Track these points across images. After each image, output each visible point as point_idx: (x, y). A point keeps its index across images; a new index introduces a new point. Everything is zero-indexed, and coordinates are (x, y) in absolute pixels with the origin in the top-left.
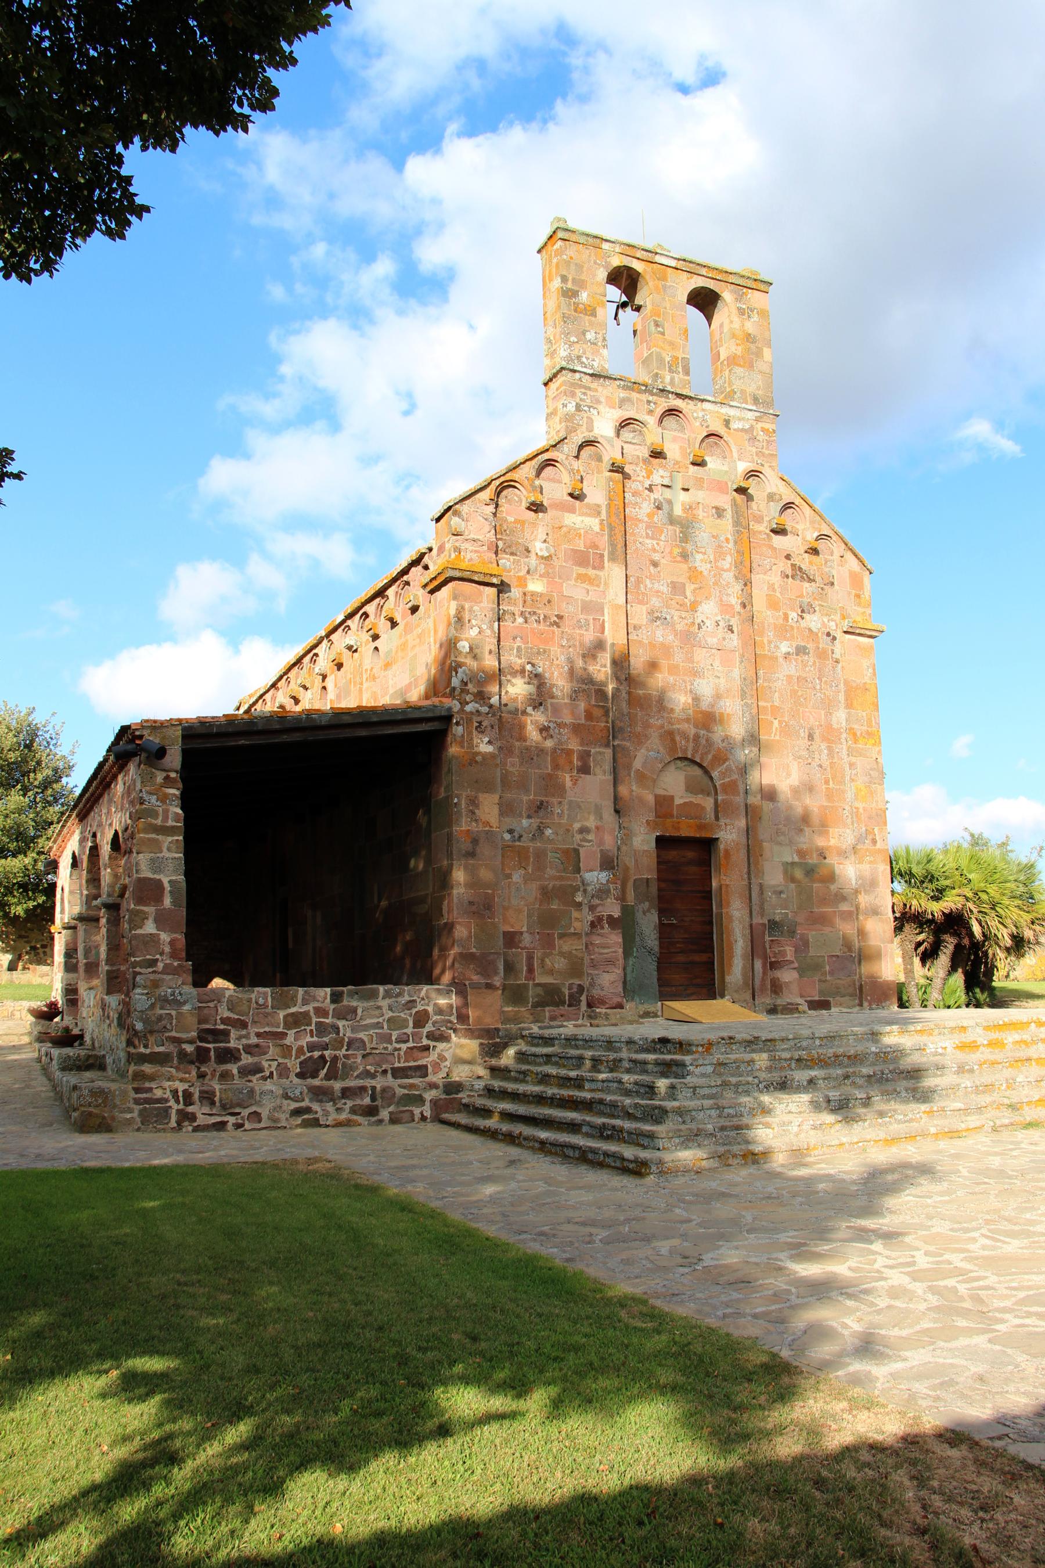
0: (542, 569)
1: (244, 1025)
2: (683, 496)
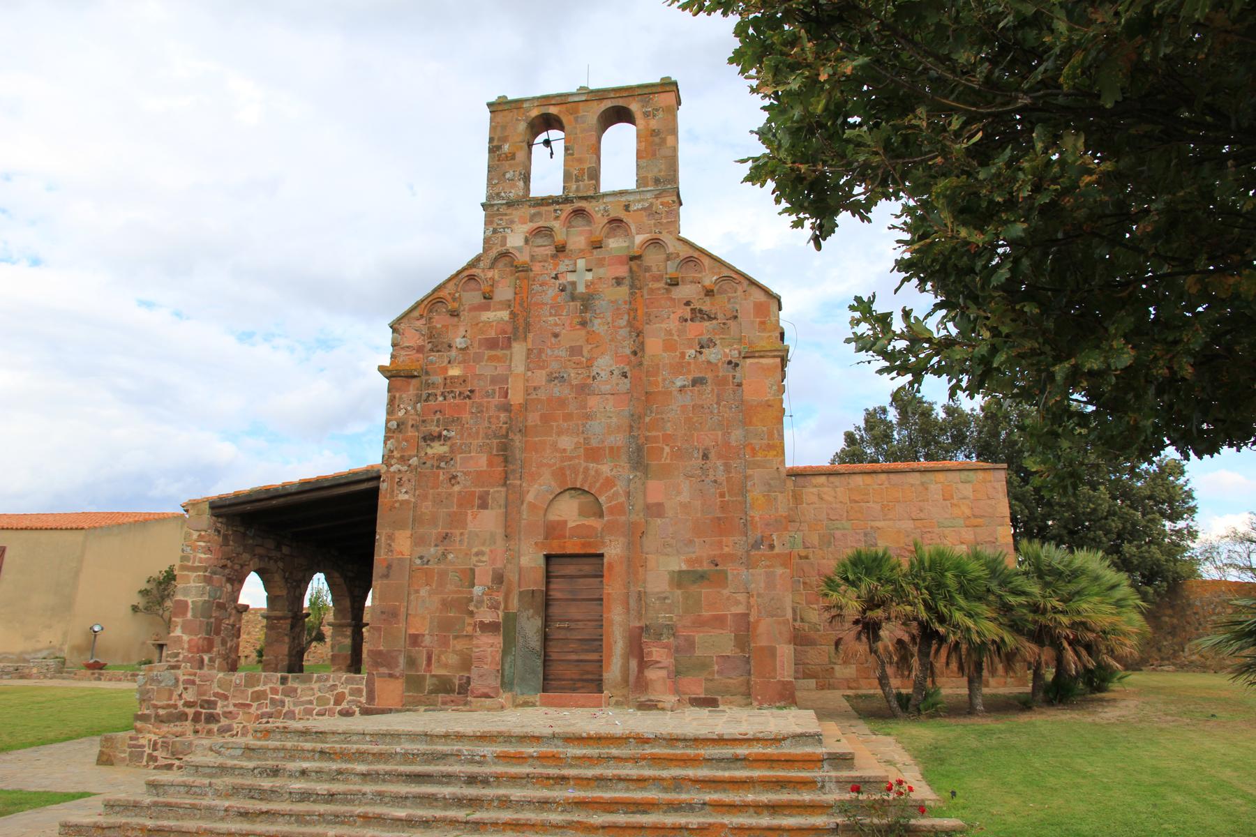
0: (460, 358)
1: (226, 698)
2: (589, 276)
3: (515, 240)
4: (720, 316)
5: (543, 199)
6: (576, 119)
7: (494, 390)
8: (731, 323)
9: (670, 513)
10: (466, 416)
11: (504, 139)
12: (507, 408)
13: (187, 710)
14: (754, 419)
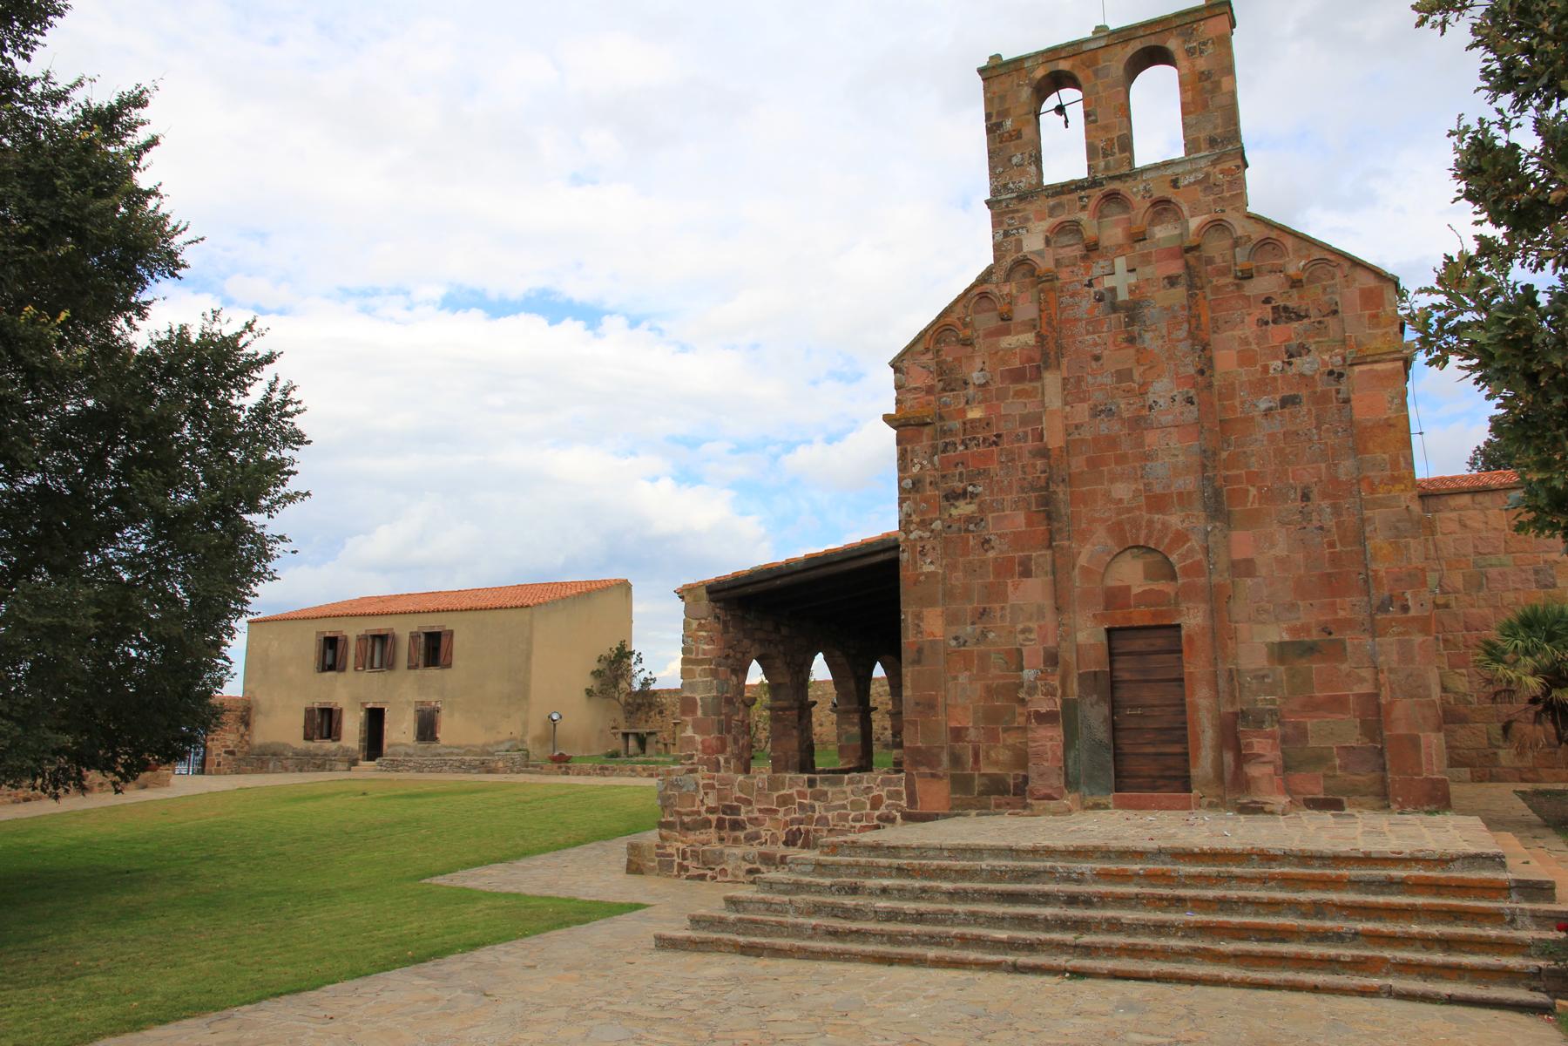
0: (980, 396)
1: (749, 803)
3: (1033, 243)
4: (1313, 312)
5: (1063, 185)
6: (1096, 73)
7: (1026, 433)
8: (1329, 320)
9: (1263, 571)
10: (994, 468)
11: (1004, 114)
12: (1044, 453)
13: (710, 816)
14: (1370, 445)
